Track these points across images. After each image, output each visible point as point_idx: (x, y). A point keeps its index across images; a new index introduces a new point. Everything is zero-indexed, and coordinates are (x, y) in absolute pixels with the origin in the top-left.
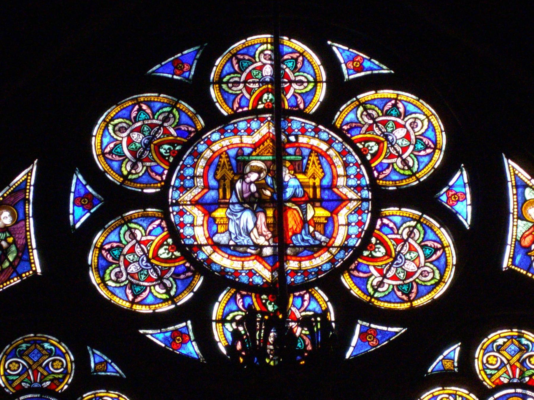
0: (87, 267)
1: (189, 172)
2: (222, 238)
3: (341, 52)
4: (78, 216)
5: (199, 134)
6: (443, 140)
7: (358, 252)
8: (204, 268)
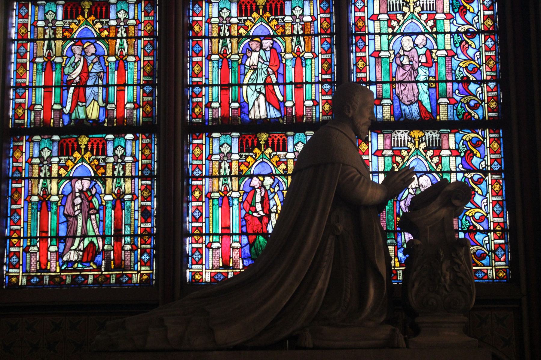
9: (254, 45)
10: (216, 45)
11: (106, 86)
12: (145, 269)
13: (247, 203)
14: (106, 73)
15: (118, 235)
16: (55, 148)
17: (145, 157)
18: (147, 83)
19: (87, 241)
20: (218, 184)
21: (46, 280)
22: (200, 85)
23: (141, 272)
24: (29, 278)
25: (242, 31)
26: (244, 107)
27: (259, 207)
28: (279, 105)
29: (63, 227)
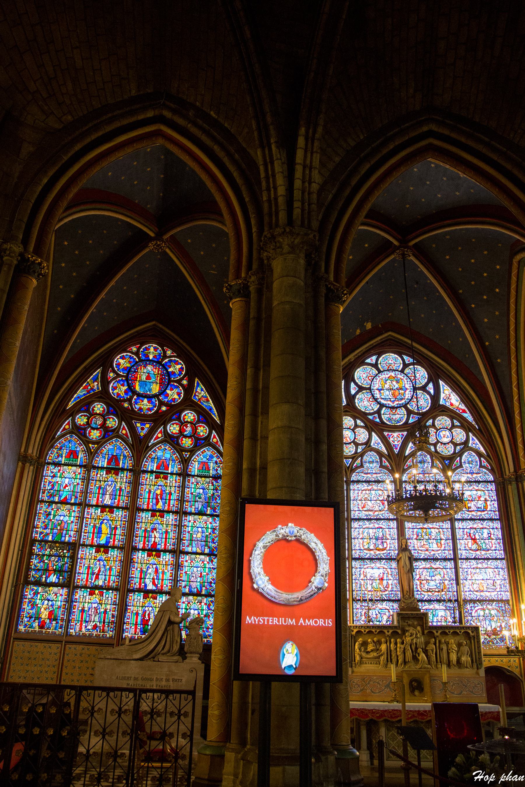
0: (355, 403)
1: (375, 383)
2: (383, 397)
3: (405, 357)
4: (353, 392)
5: (377, 375)
6: (427, 376)
7: (410, 400)
8: (379, 403)
9: (151, 566)
10: (139, 565)
11: (105, 575)
12: (111, 633)
13: (144, 615)
14: (106, 571)
15: (104, 622)
16: (88, 593)
17: (114, 598)
18: (118, 575)
19: (94, 623)
20: (136, 608)
21: (81, 634)
22: (133, 577)
23: (110, 634)
24: (76, 633)
25: (148, 562)
26: (146, 585)
27: (147, 616)
28: (156, 586)
29: (88, 618)
